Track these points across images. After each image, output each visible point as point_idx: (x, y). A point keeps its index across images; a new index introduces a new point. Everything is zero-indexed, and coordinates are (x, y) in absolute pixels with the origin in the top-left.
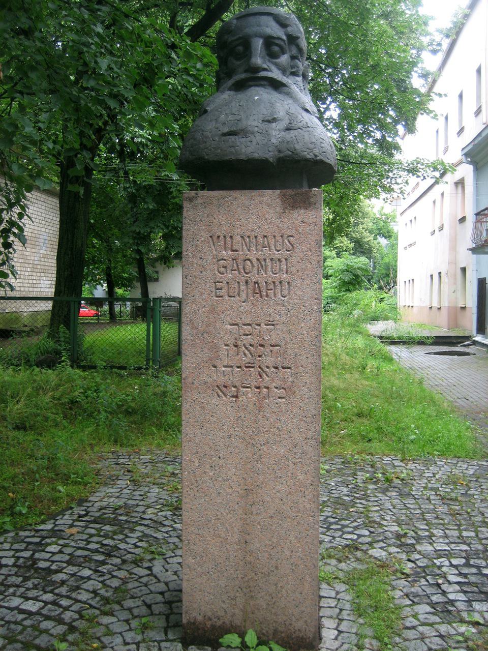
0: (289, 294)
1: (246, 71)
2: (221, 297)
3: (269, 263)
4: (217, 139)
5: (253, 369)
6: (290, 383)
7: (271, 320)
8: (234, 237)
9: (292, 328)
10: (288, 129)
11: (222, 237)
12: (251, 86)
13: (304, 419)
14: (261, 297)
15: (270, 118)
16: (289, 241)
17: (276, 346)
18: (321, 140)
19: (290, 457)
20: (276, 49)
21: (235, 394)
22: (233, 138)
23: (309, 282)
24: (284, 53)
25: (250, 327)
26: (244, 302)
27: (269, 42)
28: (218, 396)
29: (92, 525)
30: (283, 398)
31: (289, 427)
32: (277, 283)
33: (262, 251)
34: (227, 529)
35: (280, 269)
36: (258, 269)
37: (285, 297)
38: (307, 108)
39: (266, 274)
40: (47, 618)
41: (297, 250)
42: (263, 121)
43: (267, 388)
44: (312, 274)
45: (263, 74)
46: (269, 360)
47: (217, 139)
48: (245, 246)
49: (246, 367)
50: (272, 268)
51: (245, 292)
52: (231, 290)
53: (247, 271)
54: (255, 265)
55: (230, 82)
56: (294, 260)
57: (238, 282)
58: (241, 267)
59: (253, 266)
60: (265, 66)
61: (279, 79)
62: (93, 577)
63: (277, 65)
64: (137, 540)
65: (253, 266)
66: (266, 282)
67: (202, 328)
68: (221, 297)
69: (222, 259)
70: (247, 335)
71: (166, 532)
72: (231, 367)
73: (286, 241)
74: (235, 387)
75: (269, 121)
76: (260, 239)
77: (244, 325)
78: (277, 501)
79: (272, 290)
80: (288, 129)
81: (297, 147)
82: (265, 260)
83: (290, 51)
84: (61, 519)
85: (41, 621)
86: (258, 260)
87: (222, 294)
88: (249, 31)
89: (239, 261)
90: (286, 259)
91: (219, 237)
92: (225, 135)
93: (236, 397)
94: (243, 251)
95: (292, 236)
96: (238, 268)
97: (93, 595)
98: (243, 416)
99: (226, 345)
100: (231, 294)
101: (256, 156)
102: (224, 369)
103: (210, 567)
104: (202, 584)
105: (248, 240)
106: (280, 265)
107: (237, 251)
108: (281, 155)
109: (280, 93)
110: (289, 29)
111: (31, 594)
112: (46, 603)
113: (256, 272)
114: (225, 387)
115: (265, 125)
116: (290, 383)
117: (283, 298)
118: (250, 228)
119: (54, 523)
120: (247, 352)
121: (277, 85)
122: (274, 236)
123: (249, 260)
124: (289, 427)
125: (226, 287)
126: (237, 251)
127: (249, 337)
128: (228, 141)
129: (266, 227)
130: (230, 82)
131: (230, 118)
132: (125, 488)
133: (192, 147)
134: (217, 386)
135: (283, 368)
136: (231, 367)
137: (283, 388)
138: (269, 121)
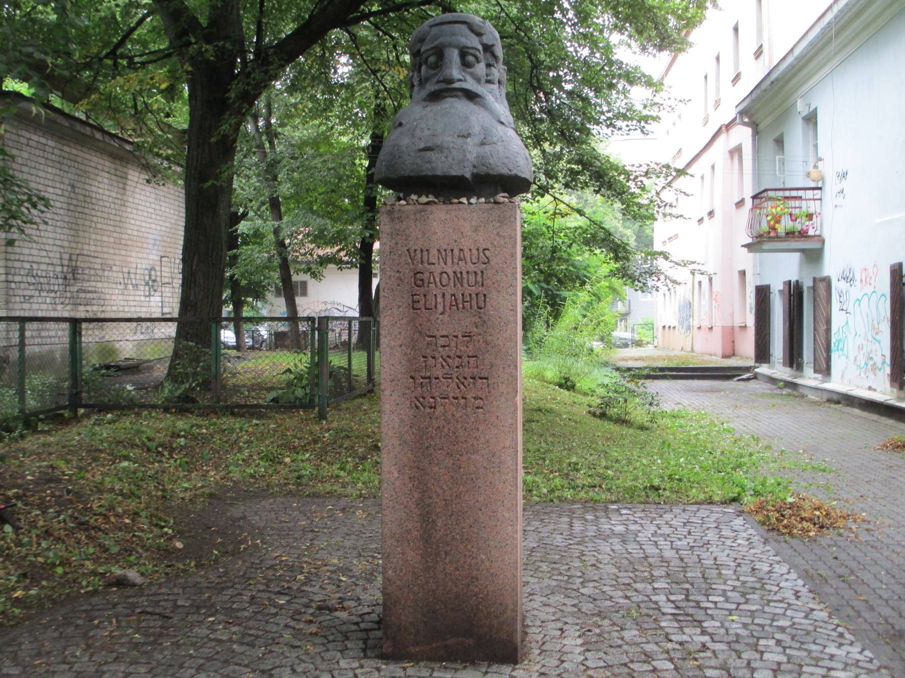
3: (465, 275)
4: (413, 154)
10: (483, 144)
11: (418, 252)
12: (445, 97)
14: (458, 309)
22: (428, 154)
24: (478, 62)
41: (492, 263)
42: (458, 136)
45: (457, 85)
50: (468, 280)
52: (428, 303)
55: (425, 93)
58: (438, 280)
59: (449, 279)
63: (472, 75)
65: (449, 279)
73: (481, 254)
74: (433, 398)
75: (463, 136)
76: (456, 252)
80: (483, 144)
81: (491, 161)
82: (461, 273)
89: (436, 275)
91: (415, 250)
108: (475, 171)
109: (475, 104)
115: (460, 141)
120: (444, 363)
121: (471, 96)
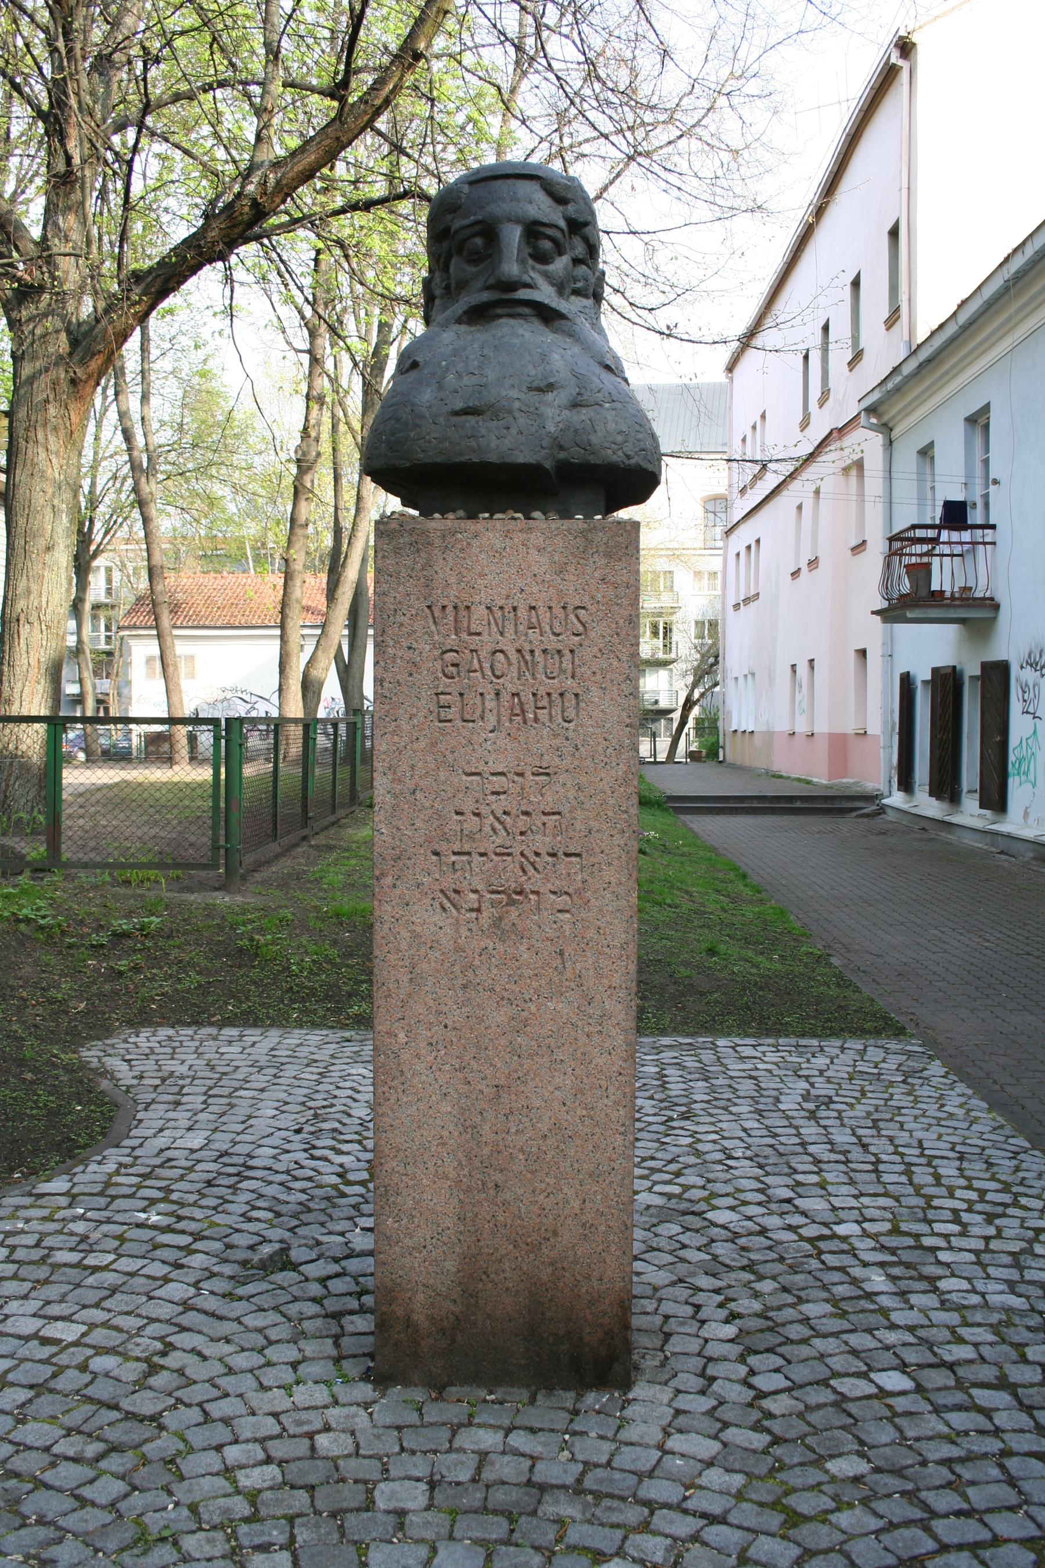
0: (577, 715)
1: (488, 288)
2: (450, 721)
3: (539, 657)
4: (442, 420)
5: (509, 858)
6: (580, 885)
7: (545, 765)
8: (473, 608)
9: (584, 780)
10: (576, 405)
11: (450, 609)
12: (500, 316)
13: (607, 950)
14: (525, 722)
15: (542, 384)
16: (577, 617)
17: (554, 814)
18: (637, 427)
19: (580, 1023)
20: (547, 245)
21: (476, 906)
22: (472, 420)
23: (615, 695)
24: (560, 254)
25: (503, 778)
26: (491, 732)
27: (533, 230)
28: (444, 909)
29: (148, 1183)
30: (567, 911)
31: (578, 966)
32: (555, 696)
33: (526, 635)
34: (460, 1163)
35: (560, 667)
36: (519, 669)
37: (570, 722)
38: (609, 363)
39: (535, 678)
40: (101, 1351)
41: (592, 634)
42: (530, 389)
43: (537, 893)
44: (621, 678)
45: (523, 294)
46: (542, 842)
47: (442, 420)
48: (493, 626)
49: (496, 854)
50: (545, 667)
51: (495, 712)
52: (468, 709)
53: (498, 673)
54: (514, 661)
55: (460, 307)
56: (587, 653)
57: (482, 694)
58: (486, 665)
59: (510, 664)
60: (526, 278)
61: (554, 305)
62: (171, 1276)
63: (547, 276)
64: (248, 1207)
65: (510, 664)
66: (534, 695)
67: (413, 782)
68: (450, 721)
69: (451, 650)
70: (498, 793)
71: (303, 1191)
72: (469, 854)
73: (572, 617)
74: (475, 891)
75: (539, 390)
76: (522, 613)
77: (493, 774)
78: (556, 1105)
79: (544, 708)
80: (576, 405)
81: (594, 439)
82: (532, 652)
83: (573, 248)
84: (83, 1172)
85: (91, 1357)
86: (519, 651)
87: (449, 717)
88: (497, 209)
89: (483, 654)
90: (572, 651)
91: (444, 607)
92: (457, 413)
93: (478, 910)
94: (490, 635)
95: (583, 608)
96: (481, 668)
97: (180, 1309)
98: (491, 947)
99: (457, 813)
100: (468, 717)
101: (521, 459)
102: (454, 858)
103: (428, 1237)
104: (412, 1268)
105: (500, 613)
106: (561, 662)
107: (479, 634)
108: (562, 455)
109: (556, 331)
110: (571, 207)
111: (55, 1310)
112: (92, 1326)
113: (515, 674)
114: (456, 891)
115: (534, 398)
116: (580, 885)
117: (566, 725)
118: (503, 592)
119: (70, 1180)
120: (498, 826)
121: (548, 316)
122: (550, 608)
123: (502, 651)
124: (578, 966)
125: (458, 704)
126: (479, 634)
127: (502, 797)
128: (463, 426)
129: (535, 589)
130: (460, 307)
131: (466, 380)
132: (202, 1111)
133: (393, 434)
134: (442, 891)
135: (567, 855)
136: (469, 854)
137: (566, 893)
138: (539, 390)
